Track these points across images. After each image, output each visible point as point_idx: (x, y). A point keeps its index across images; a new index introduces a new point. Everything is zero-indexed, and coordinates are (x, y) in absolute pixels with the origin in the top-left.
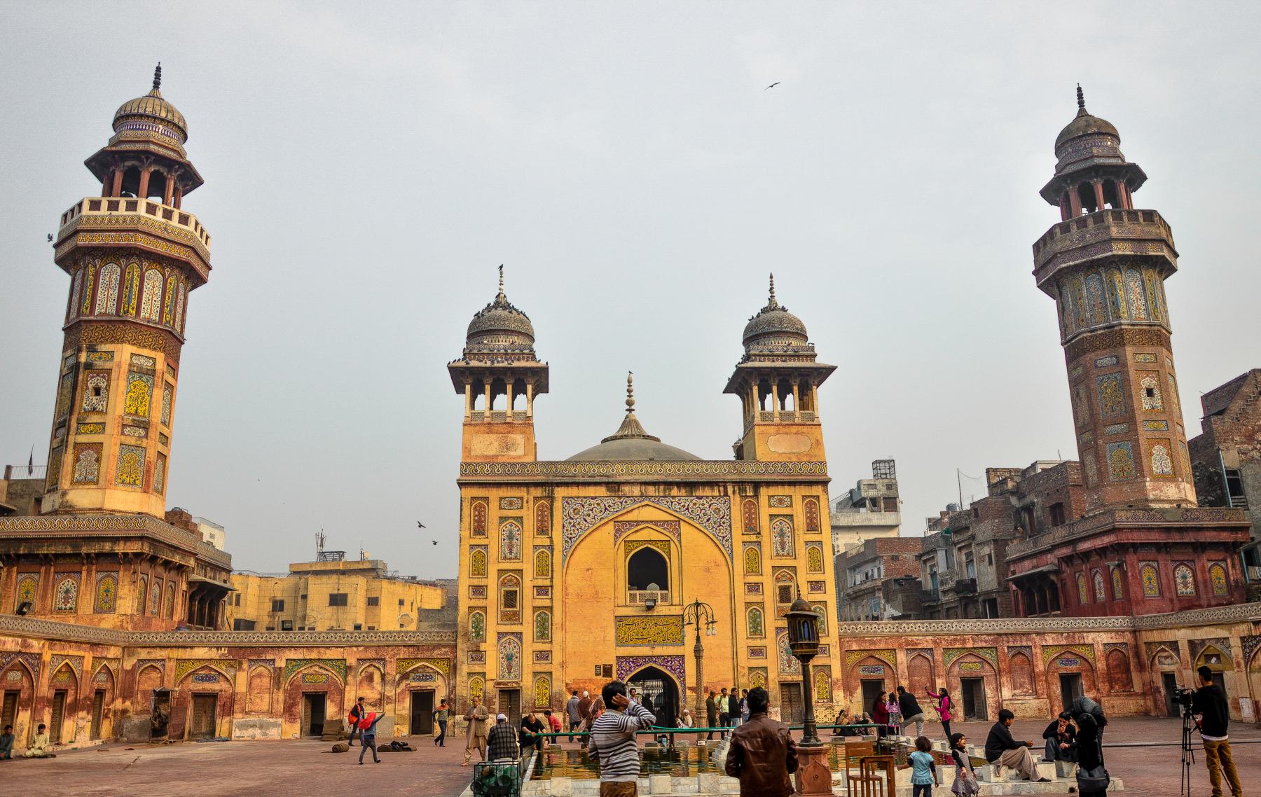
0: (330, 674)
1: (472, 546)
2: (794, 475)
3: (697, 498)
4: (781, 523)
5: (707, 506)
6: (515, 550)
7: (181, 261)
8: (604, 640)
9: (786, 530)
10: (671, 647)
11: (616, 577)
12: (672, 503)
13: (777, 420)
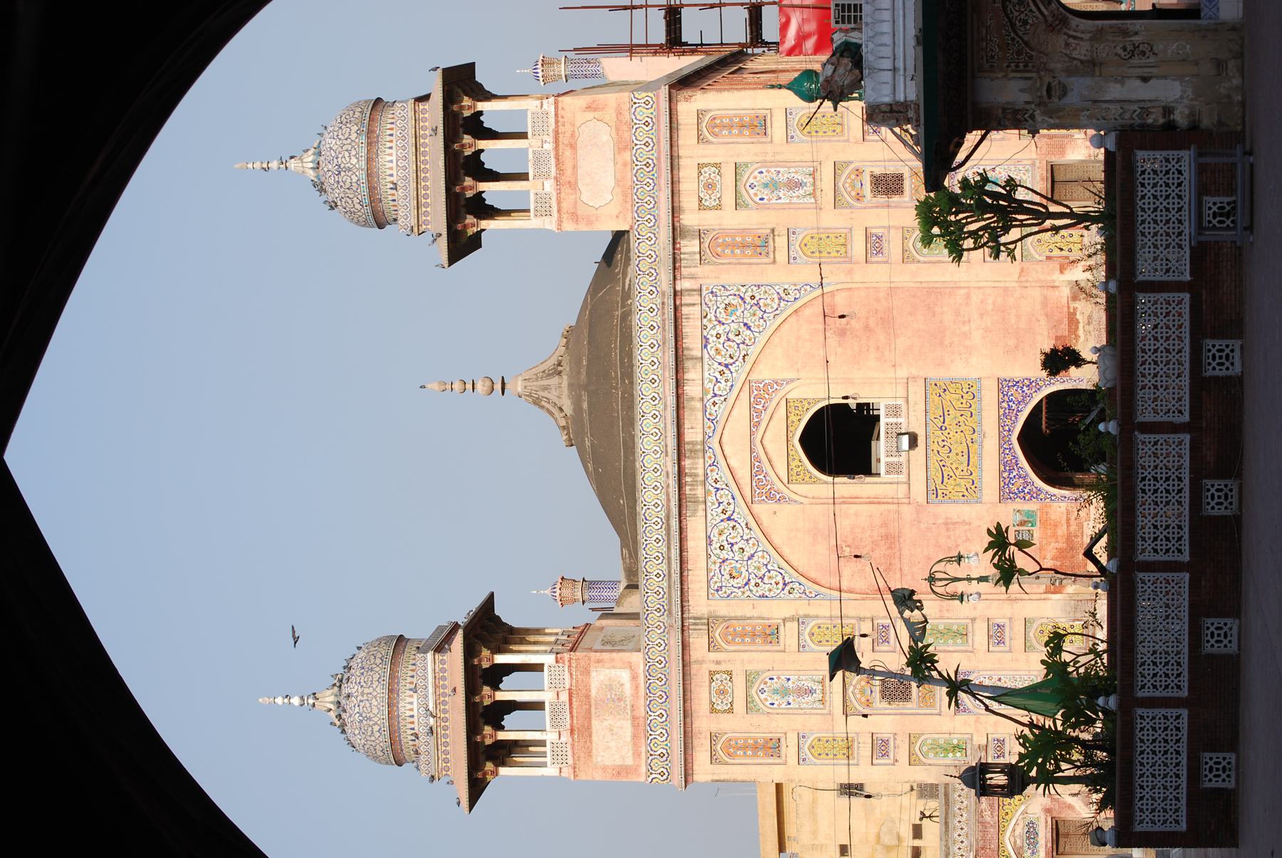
1: (801, 760)
2: (658, 159)
3: (706, 347)
4: (752, 186)
5: (720, 329)
6: (811, 684)
8: (970, 524)
9: (765, 178)
10: (985, 402)
11: (853, 500)
12: (715, 395)
13: (549, 186)
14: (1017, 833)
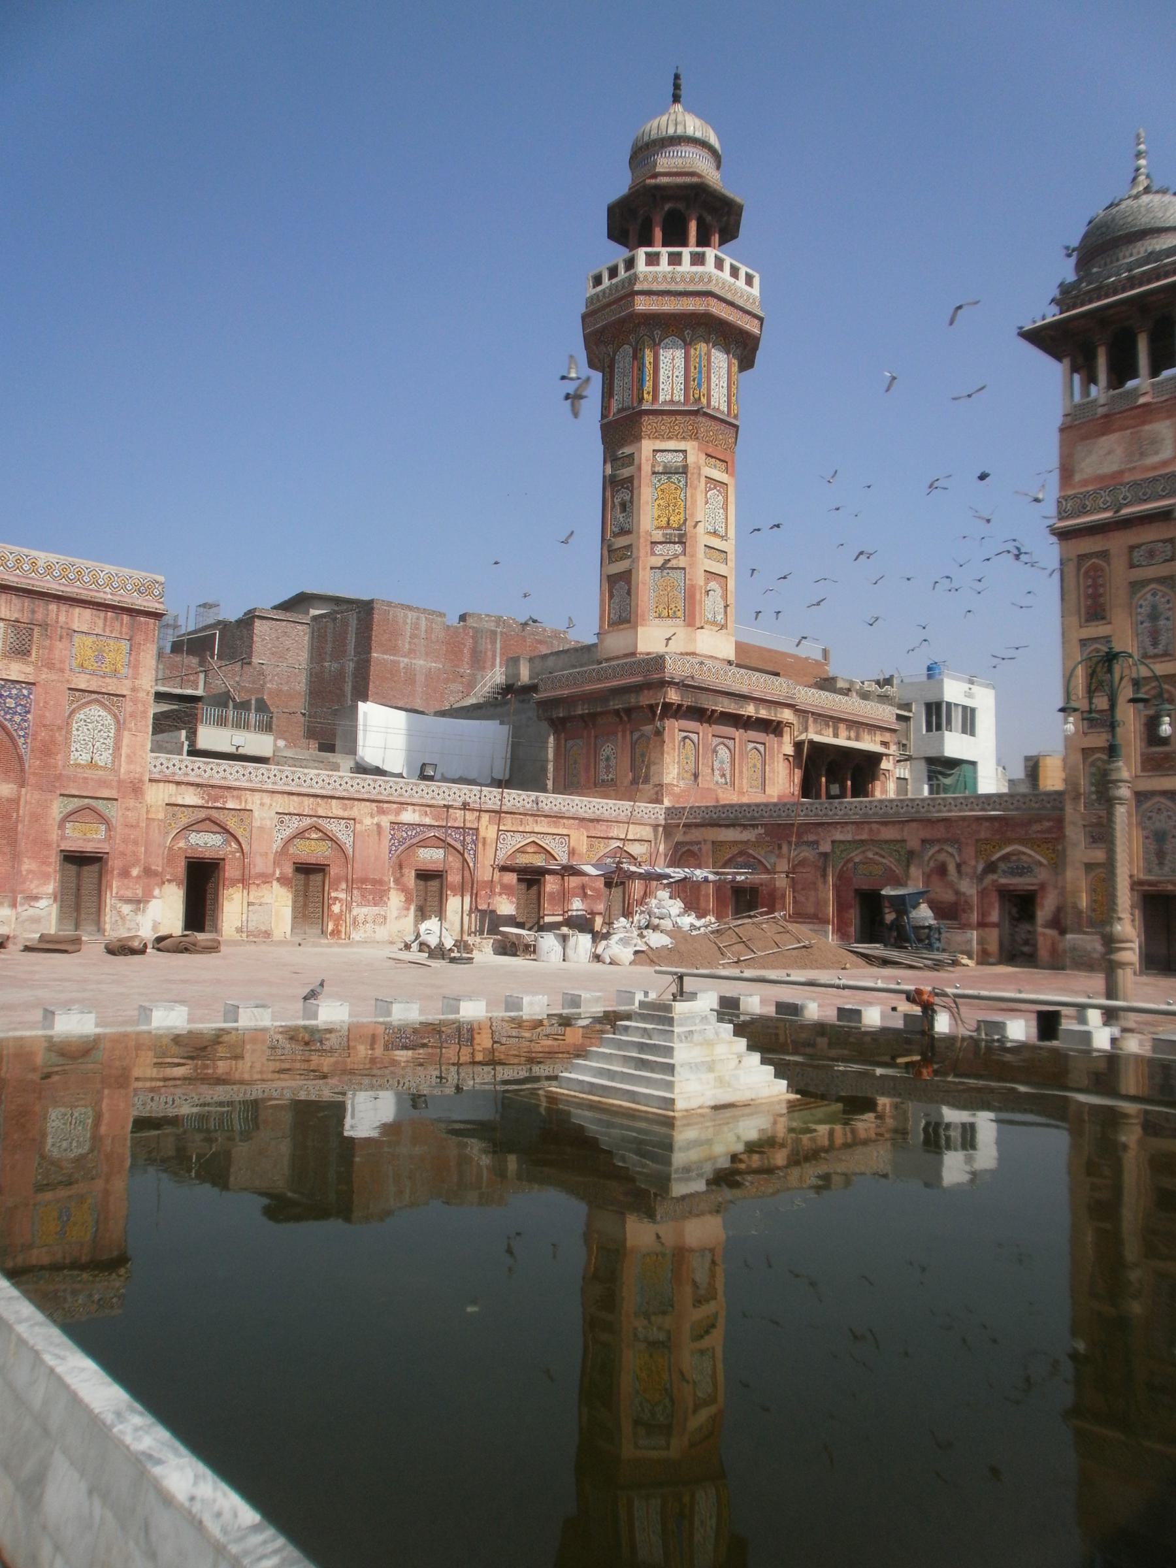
0: (888, 864)
1: (1083, 642)
7: (699, 314)
14: (1024, 857)
